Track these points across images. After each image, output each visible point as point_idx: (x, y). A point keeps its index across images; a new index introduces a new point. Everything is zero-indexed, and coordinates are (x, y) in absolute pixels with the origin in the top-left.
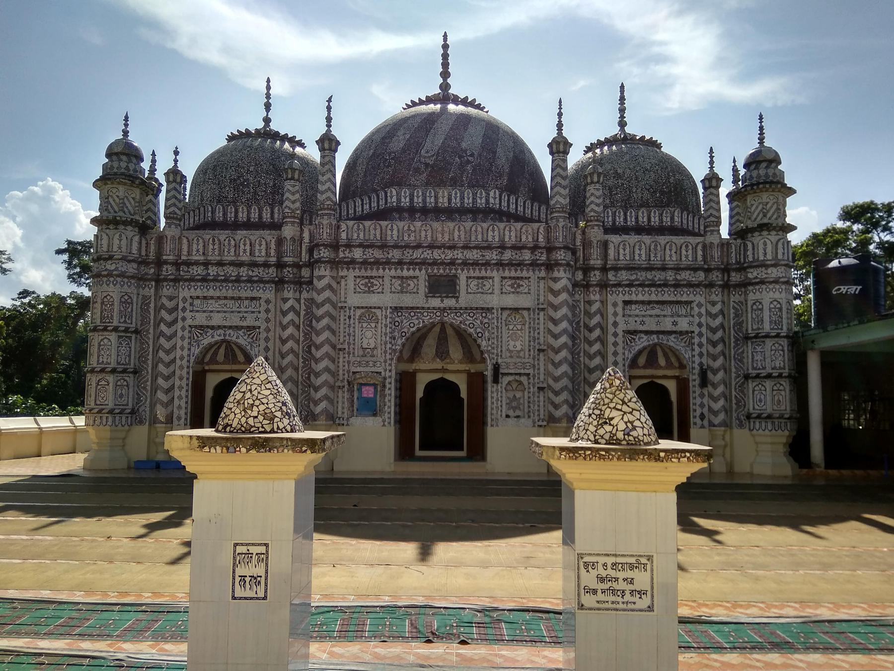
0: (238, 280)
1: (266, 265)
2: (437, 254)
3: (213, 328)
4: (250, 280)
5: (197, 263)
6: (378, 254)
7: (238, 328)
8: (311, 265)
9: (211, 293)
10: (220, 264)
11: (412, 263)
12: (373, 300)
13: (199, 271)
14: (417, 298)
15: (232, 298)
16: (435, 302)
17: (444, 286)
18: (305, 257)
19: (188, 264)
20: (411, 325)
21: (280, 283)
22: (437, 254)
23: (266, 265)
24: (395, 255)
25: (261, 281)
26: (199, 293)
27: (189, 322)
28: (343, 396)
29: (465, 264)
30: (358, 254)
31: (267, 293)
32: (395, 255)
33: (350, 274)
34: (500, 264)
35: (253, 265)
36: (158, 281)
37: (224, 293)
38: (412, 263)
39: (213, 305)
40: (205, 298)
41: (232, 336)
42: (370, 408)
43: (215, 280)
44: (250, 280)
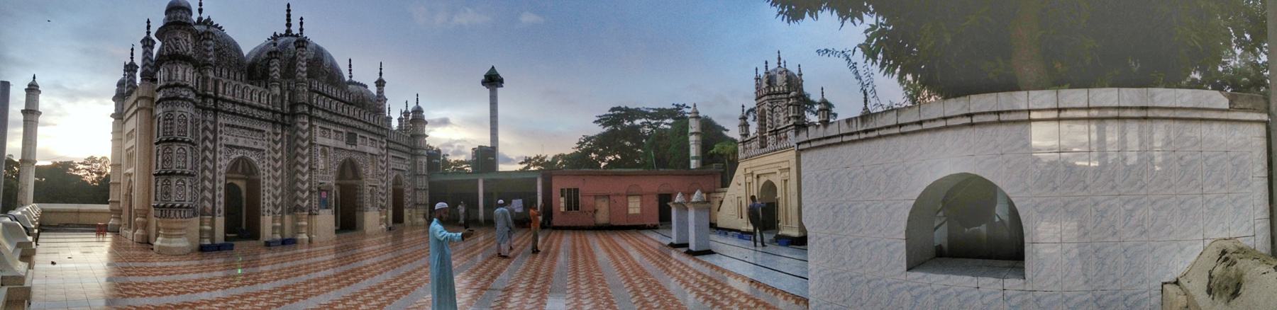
0: (253, 118)
1: (268, 110)
2: (349, 122)
3: (237, 147)
4: (259, 119)
5: (229, 101)
6: (327, 116)
7: (252, 149)
8: (294, 115)
9: (237, 123)
10: (243, 104)
11: (342, 125)
12: (327, 142)
13: (229, 106)
14: (342, 144)
15: (249, 129)
16: (349, 147)
17: (351, 139)
18: (287, 110)
19: (224, 100)
20: (342, 157)
21: (274, 123)
22: (349, 122)
23: (268, 110)
24: (334, 118)
25: (266, 120)
26: (230, 122)
27: (224, 141)
28: (316, 197)
29: (360, 129)
30: (320, 114)
31: (268, 129)
32: (334, 118)
33: (317, 124)
34: (369, 132)
35: (261, 109)
36: (205, 109)
37: (244, 124)
38: (342, 125)
39: (237, 132)
40: (233, 126)
41: (249, 154)
42: (325, 204)
43: (241, 115)
44: (259, 119)
